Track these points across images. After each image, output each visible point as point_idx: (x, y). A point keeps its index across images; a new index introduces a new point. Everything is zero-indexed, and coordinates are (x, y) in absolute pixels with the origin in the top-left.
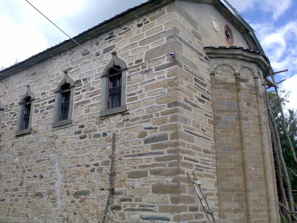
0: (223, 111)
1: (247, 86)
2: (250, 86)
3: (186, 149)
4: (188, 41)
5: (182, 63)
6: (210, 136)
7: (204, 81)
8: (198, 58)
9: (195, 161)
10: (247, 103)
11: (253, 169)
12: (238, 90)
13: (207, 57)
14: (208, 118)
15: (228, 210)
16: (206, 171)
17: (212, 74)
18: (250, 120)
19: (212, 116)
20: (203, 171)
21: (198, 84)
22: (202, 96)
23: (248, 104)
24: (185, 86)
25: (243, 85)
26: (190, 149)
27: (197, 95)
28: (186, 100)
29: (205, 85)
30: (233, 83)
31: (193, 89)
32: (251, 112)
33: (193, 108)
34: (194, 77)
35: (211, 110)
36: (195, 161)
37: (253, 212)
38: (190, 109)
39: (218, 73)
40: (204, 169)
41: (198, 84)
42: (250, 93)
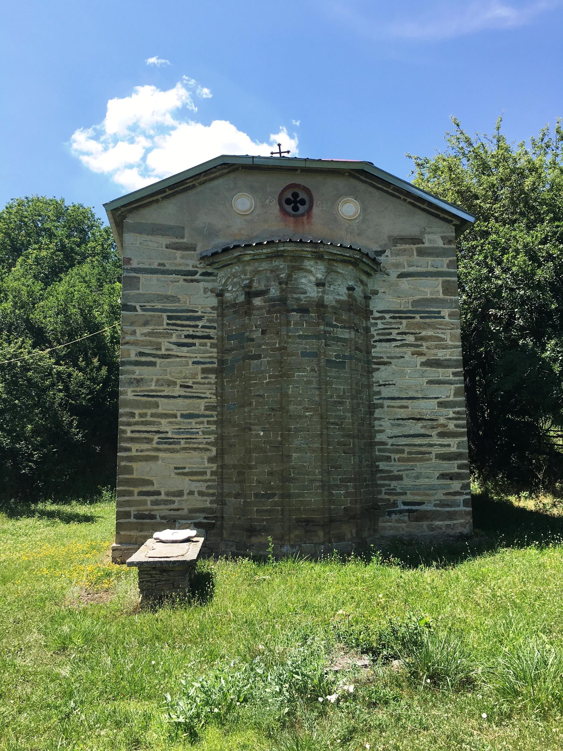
0: (230, 350)
1: (265, 302)
2: (271, 300)
3: (137, 419)
4: (155, 266)
5: (133, 304)
6: (205, 393)
7: (197, 312)
8: (182, 282)
9: (158, 432)
10: (262, 330)
11: (262, 434)
12: (248, 313)
13: (210, 270)
14: (200, 367)
15: (229, 495)
16: (186, 443)
17: (220, 295)
18: (264, 358)
19: (215, 360)
20: (179, 443)
21: (179, 322)
22: (187, 337)
23: (263, 332)
24: (142, 334)
25: (257, 302)
26: (149, 418)
27: (174, 339)
28: (141, 354)
29: (200, 318)
30: (242, 303)
31: (161, 333)
32: (267, 344)
33: (158, 361)
34: (165, 315)
35: (212, 352)
36: (158, 432)
37: (255, 498)
38: (153, 364)
39: (228, 291)
40: (182, 442)
41: (179, 322)
42: (269, 312)
